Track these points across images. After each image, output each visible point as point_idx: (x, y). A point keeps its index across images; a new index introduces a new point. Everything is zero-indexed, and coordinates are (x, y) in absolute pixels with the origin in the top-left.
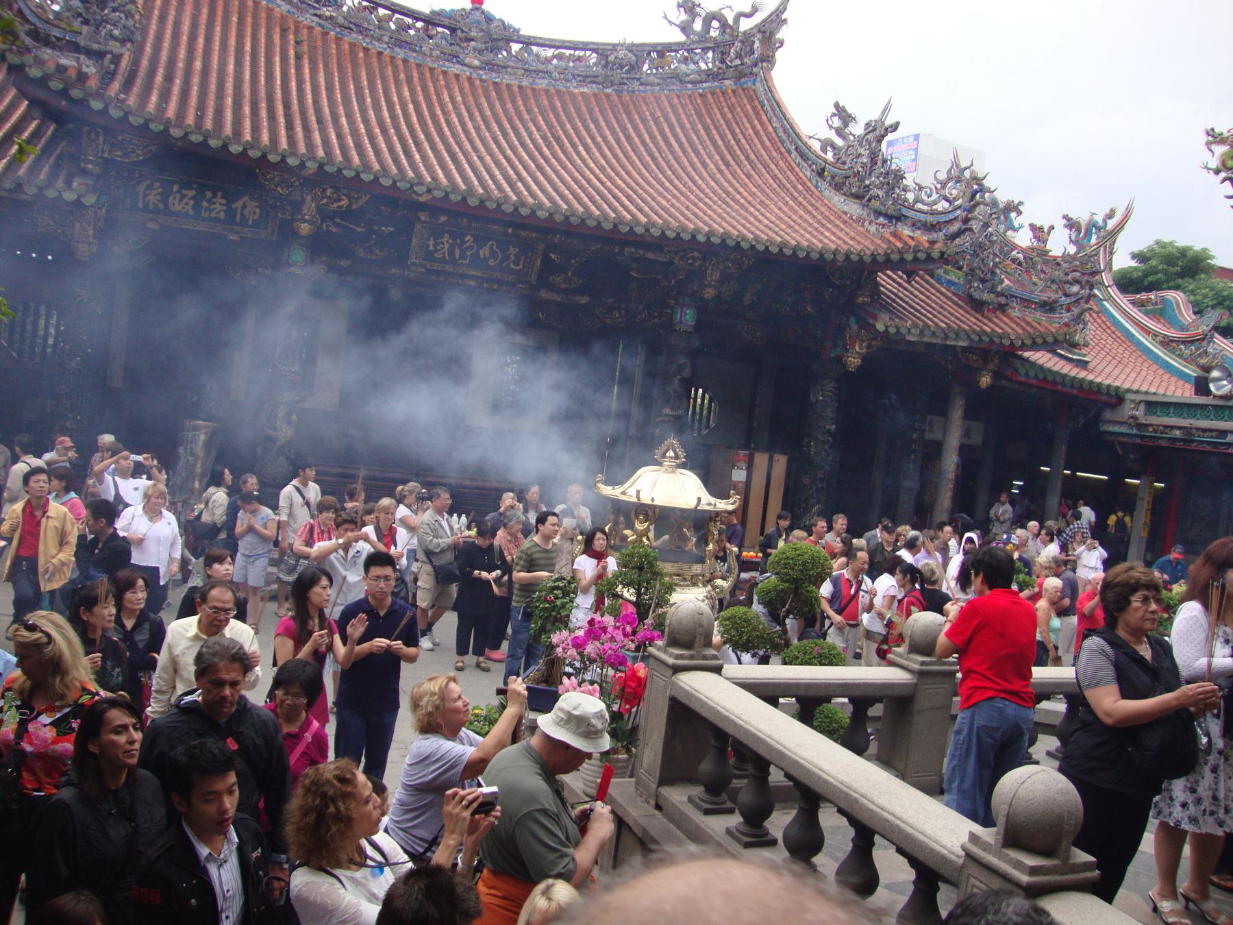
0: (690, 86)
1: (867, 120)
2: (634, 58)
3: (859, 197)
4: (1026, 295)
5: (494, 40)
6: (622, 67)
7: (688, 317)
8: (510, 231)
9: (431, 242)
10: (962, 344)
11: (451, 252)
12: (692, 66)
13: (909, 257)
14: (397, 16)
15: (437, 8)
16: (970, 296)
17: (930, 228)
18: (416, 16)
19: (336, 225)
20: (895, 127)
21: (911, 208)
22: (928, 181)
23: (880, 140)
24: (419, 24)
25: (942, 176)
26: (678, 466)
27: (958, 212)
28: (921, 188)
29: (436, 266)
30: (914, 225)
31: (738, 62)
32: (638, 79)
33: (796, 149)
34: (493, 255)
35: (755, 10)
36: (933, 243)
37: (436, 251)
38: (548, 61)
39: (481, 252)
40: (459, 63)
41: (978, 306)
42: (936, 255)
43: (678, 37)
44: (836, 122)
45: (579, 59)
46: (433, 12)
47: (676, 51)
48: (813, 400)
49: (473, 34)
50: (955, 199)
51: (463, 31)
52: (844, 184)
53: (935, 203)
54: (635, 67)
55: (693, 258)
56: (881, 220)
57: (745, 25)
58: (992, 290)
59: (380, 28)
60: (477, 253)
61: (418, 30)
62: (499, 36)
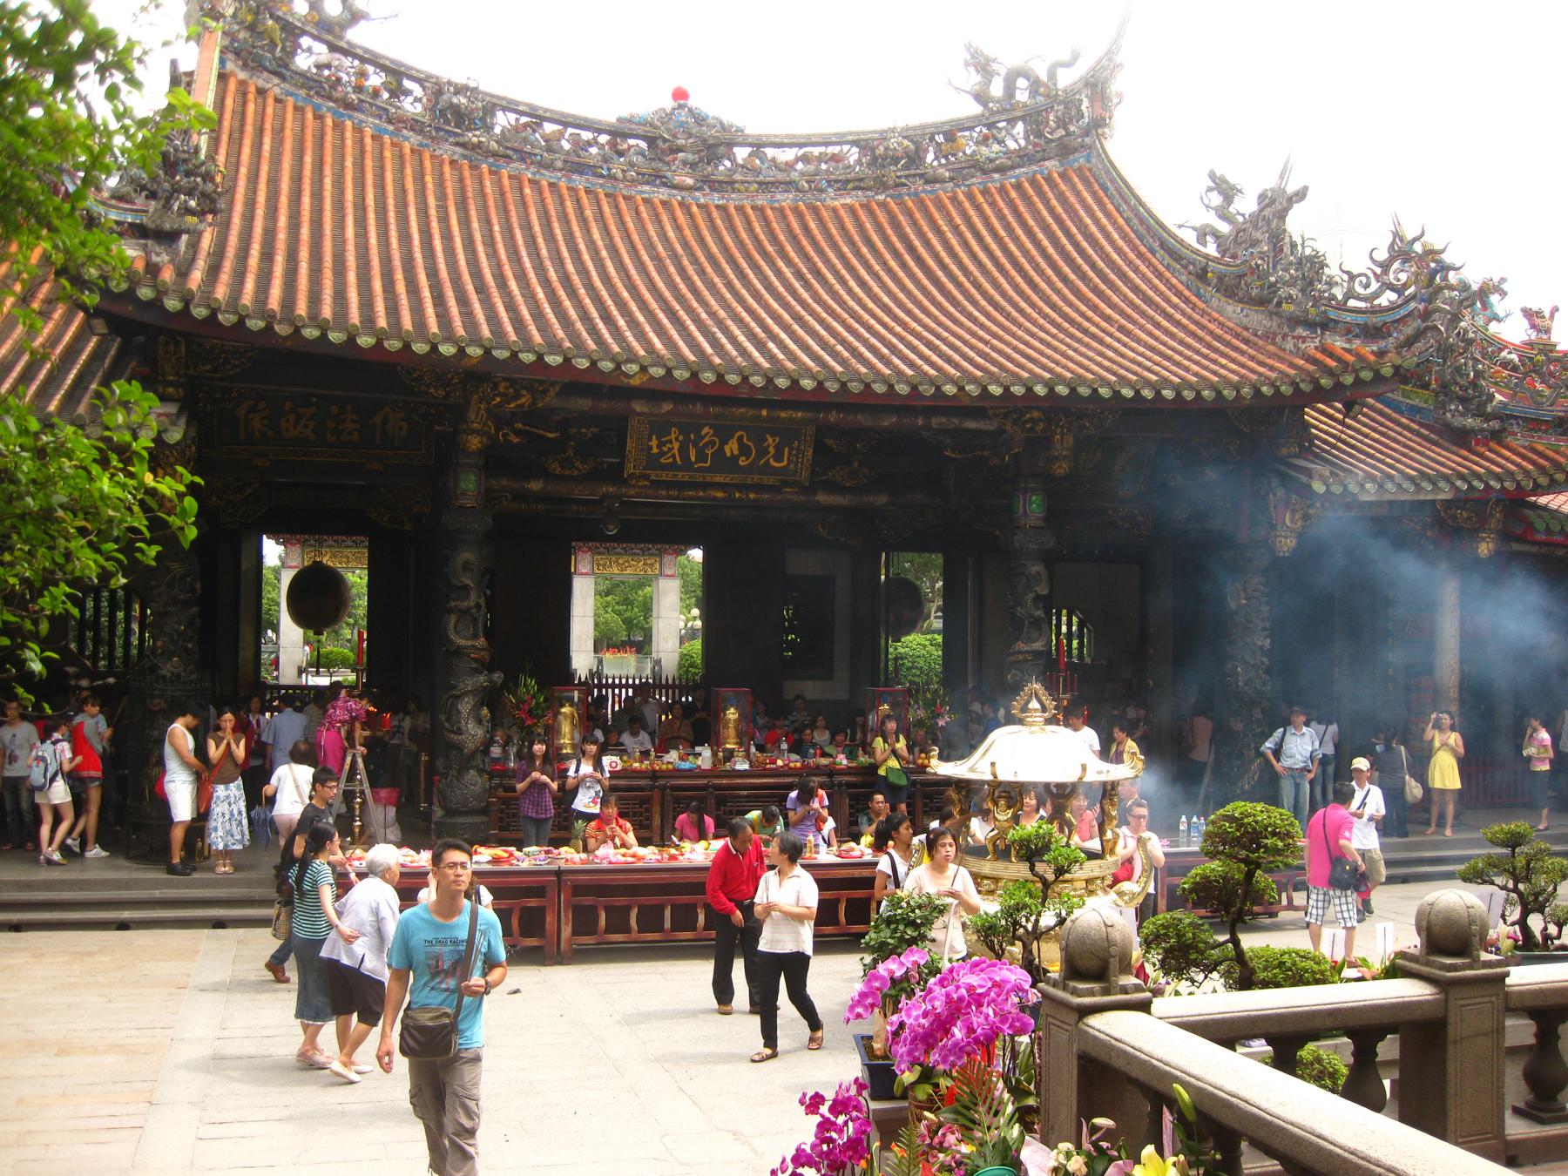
0: (996, 176)
1: (1259, 191)
2: (912, 147)
3: (1261, 302)
4: (1532, 413)
5: (710, 147)
6: (896, 160)
7: (1033, 507)
8: (764, 413)
9: (654, 443)
10: (1442, 496)
11: (683, 451)
12: (996, 147)
13: (1348, 379)
14: (570, 130)
15: (625, 114)
16: (1447, 425)
17: (1372, 332)
18: (598, 129)
19: (518, 433)
20: (1301, 195)
21: (1342, 307)
22: (1360, 265)
23: (1282, 215)
24: (603, 138)
25: (1382, 255)
26: (1048, 722)
27: (1413, 305)
28: (1352, 277)
29: (665, 476)
30: (1348, 331)
31: (1061, 132)
32: (922, 176)
33: (1163, 245)
34: (744, 451)
36: (1381, 354)
37: (663, 454)
38: (790, 166)
39: (727, 449)
40: (664, 185)
41: (1460, 438)
42: (1387, 371)
44: (1216, 199)
45: (835, 158)
46: (619, 120)
47: (971, 129)
48: (1233, 606)
49: (681, 142)
52: (1238, 286)
53: (1377, 295)
54: (915, 158)
55: (1032, 420)
56: (1300, 331)
57: (1065, 79)
58: (1480, 413)
59: (549, 150)
60: (721, 451)
61: (602, 147)
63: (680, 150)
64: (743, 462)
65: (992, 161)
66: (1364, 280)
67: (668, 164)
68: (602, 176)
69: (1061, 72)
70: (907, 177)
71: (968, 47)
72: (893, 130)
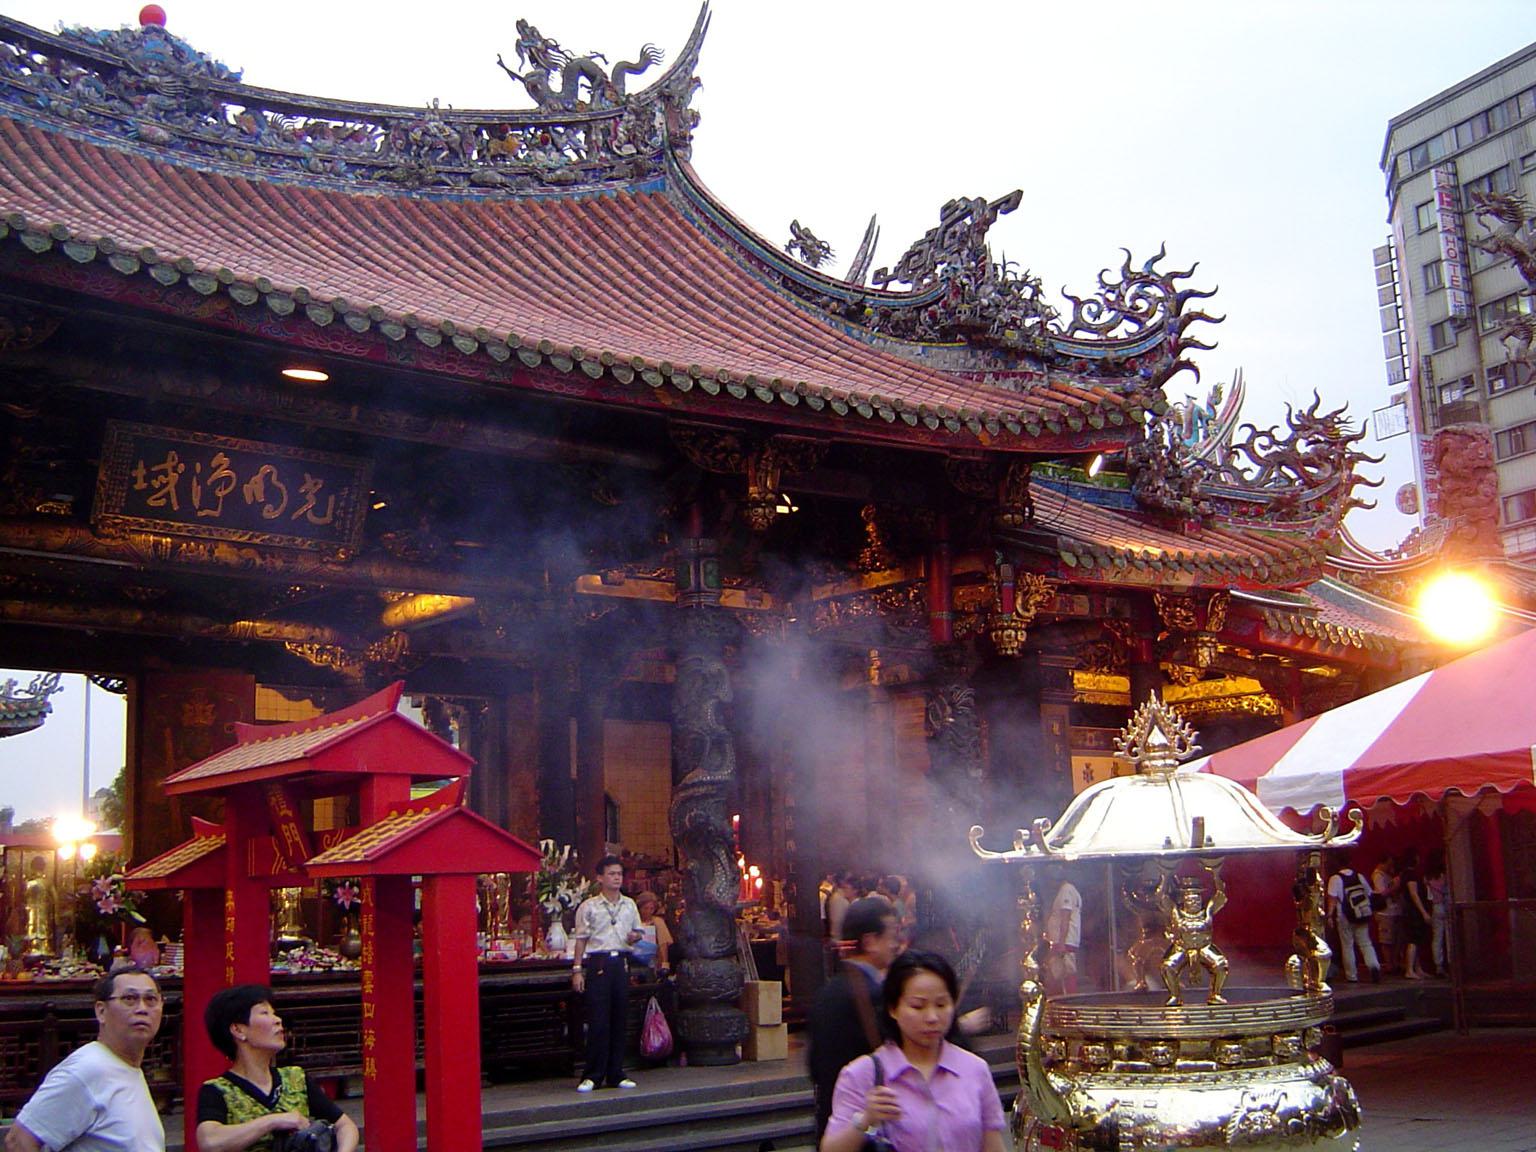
0: (557, 189)
9: (140, 472)
11: (184, 488)
12: (554, 155)
17: (1109, 370)
20: (1011, 202)
22: (1088, 290)
24: (39, 58)
25: (1114, 277)
27: (1160, 336)
28: (1078, 304)
31: (629, 149)
35: (647, 59)
37: (151, 491)
38: (298, 135)
43: (520, 100)
46: (65, 34)
47: (524, 127)
50: (1149, 314)
51: (131, 72)
56: (1027, 366)
57: (634, 85)
60: (239, 489)
62: (204, 88)
63: (151, 89)
64: (270, 513)
65: (551, 170)
66: (1094, 308)
67: (132, 105)
68: (39, 107)
69: (629, 78)
70: (449, 173)
71: (521, 25)
72: (435, 110)
